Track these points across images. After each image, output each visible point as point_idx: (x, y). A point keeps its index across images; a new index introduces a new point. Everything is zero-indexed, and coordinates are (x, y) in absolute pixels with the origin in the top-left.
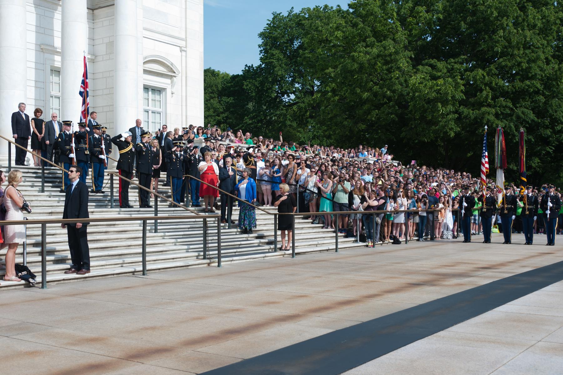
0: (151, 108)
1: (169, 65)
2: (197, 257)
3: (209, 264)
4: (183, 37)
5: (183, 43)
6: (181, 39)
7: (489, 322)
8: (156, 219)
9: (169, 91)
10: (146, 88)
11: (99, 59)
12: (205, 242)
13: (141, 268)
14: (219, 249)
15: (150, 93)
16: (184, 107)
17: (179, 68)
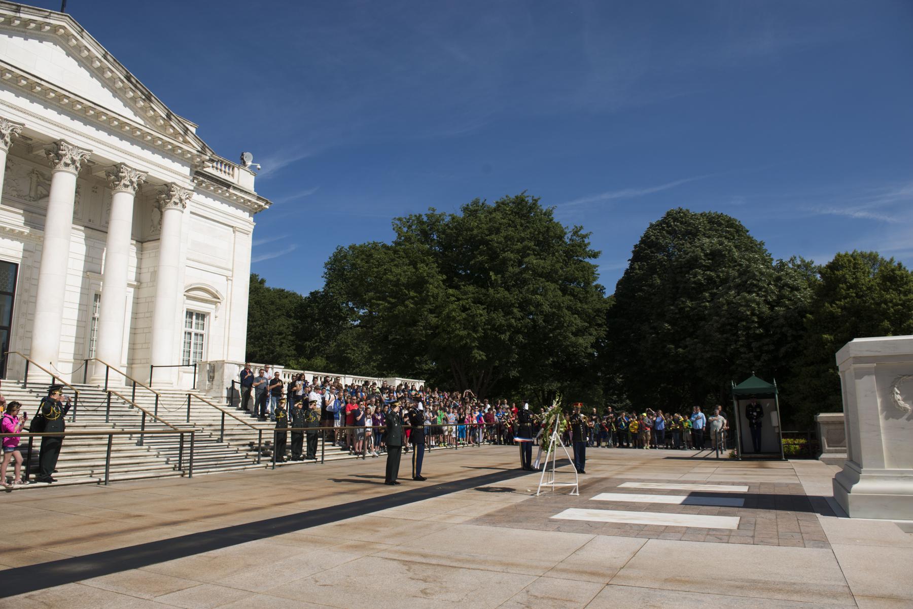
0: (194, 330)
1: (214, 292)
2: (174, 469)
3: (182, 475)
4: (231, 268)
5: (229, 274)
6: (229, 270)
7: (340, 525)
8: (142, 433)
9: (212, 316)
10: (190, 314)
11: (144, 285)
12: (181, 455)
13: (103, 479)
14: (191, 461)
15: (194, 317)
16: (227, 330)
17: (224, 295)
